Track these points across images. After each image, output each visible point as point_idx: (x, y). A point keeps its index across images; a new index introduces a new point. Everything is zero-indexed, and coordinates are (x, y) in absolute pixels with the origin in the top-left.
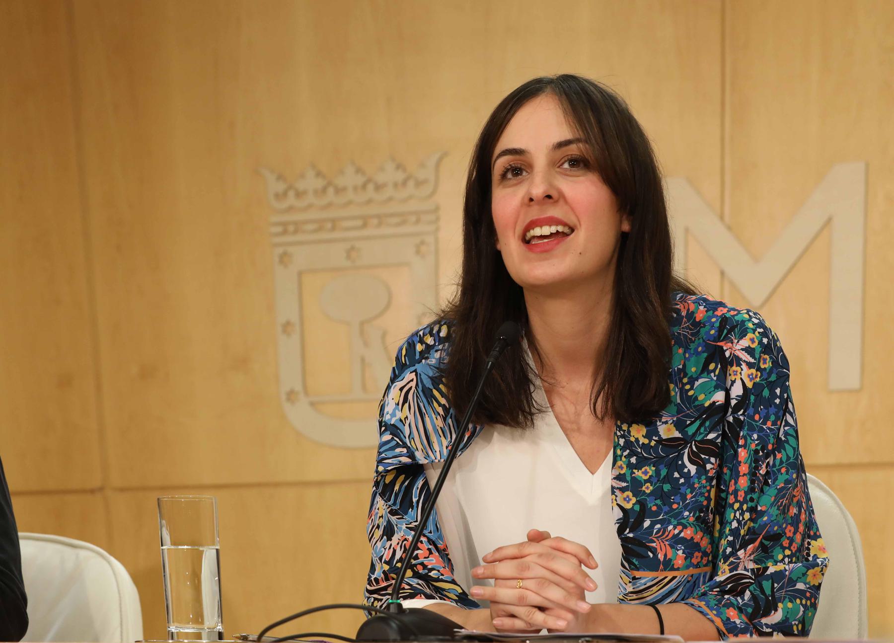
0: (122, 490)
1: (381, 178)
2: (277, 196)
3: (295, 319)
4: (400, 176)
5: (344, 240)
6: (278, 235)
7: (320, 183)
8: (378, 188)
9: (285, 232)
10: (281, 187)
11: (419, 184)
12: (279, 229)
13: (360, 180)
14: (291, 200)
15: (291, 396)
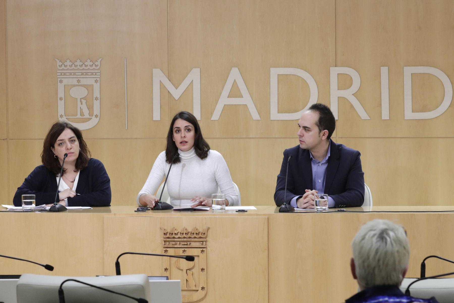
0: (12, 139)
1: (86, 63)
3: (63, 97)
4: (91, 63)
6: (59, 75)
7: (71, 64)
9: (61, 75)
10: (61, 64)
12: (60, 74)
13: (81, 63)
14: (63, 67)
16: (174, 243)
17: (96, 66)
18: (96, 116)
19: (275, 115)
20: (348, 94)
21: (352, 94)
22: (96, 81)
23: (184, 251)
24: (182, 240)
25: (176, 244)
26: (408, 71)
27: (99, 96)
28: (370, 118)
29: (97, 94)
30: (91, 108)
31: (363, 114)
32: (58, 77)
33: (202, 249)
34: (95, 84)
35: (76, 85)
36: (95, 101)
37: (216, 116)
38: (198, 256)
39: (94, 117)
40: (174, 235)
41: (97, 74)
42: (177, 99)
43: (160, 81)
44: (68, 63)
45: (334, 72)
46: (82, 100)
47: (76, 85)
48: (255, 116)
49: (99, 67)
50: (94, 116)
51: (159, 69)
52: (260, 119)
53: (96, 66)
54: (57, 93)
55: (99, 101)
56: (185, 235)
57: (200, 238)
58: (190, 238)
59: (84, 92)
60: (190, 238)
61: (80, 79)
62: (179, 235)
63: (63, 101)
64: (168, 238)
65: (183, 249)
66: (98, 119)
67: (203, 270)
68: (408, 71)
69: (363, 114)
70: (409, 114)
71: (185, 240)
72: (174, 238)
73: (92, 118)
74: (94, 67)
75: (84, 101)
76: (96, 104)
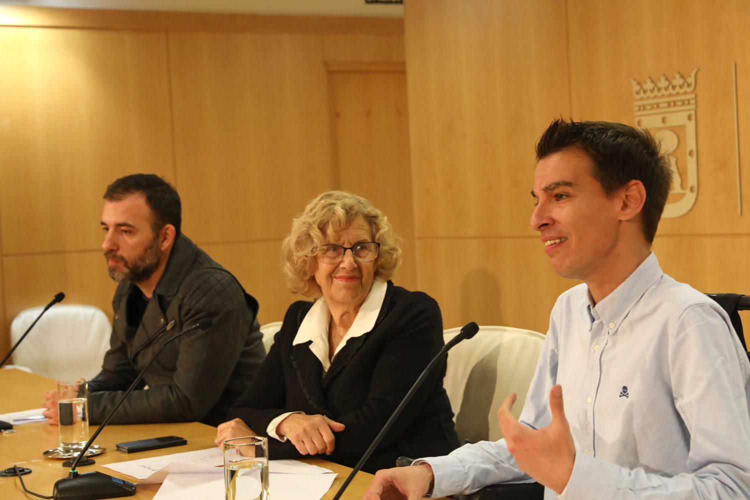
5: (661, 113)
9: (640, 110)
11: (689, 85)
12: (637, 108)
14: (642, 95)
17: (689, 85)
18: (692, 189)
22: (689, 117)
27: (694, 149)
29: (691, 144)
32: (636, 114)
34: (687, 122)
36: (689, 158)
50: (689, 190)
55: (694, 158)
61: (666, 115)
66: (695, 194)
74: (686, 88)
76: (691, 164)
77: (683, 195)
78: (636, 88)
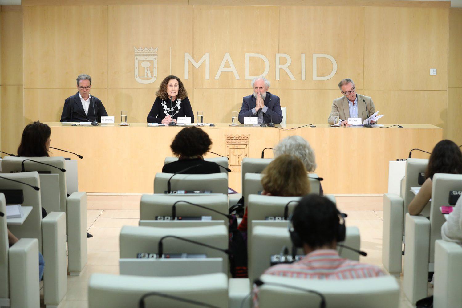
0: (110, 88)
2: (136, 51)
3: (137, 66)
4: (153, 50)
8: (150, 51)
9: (137, 55)
10: (137, 49)
13: (147, 50)
15: (137, 77)
16: (232, 142)
19: (247, 77)
20: (285, 67)
21: (287, 67)
22: (155, 59)
23: (237, 146)
24: (237, 140)
25: (233, 143)
26: (315, 56)
28: (295, 79)
29: (155, 65)
30: (152, 73)
31: (292, 78)
33: (246, 145)
35: (145, 61)
36: (154, 69)
37: (217, 78)
38: (244, 149)
39: (153, 77)
40: (232, 138)
41: (156, 55)
42: (197, 68)
43: (189, 59)
44: (140, 49)
45: (278, 56)
46: (148, 68)
47: (145, 61)
48: (237, 77)
49: (156, 52)
51: (188, 53)
52: (239, 79)
53: (155, 51)
54: (134, 65)
56: (237, 138)
57: (245, 139)
58: (240, 139)
59: (149, 64)
60: (240, 139)
62: (235, 138)
63: (138, 69)
64: (229, 139)
65: (237, 145)
66: (156, 78)
67: (246, 155)
68: (315, 56)
69: (292, 78)
70: (315, 78)
71: (238, 140)
72: (232, 139)
73: (152, 78)
74: (154, 52)
75: (149, 69)
76: (155, 71)
77: (151, 78)
78: (136, 49)
